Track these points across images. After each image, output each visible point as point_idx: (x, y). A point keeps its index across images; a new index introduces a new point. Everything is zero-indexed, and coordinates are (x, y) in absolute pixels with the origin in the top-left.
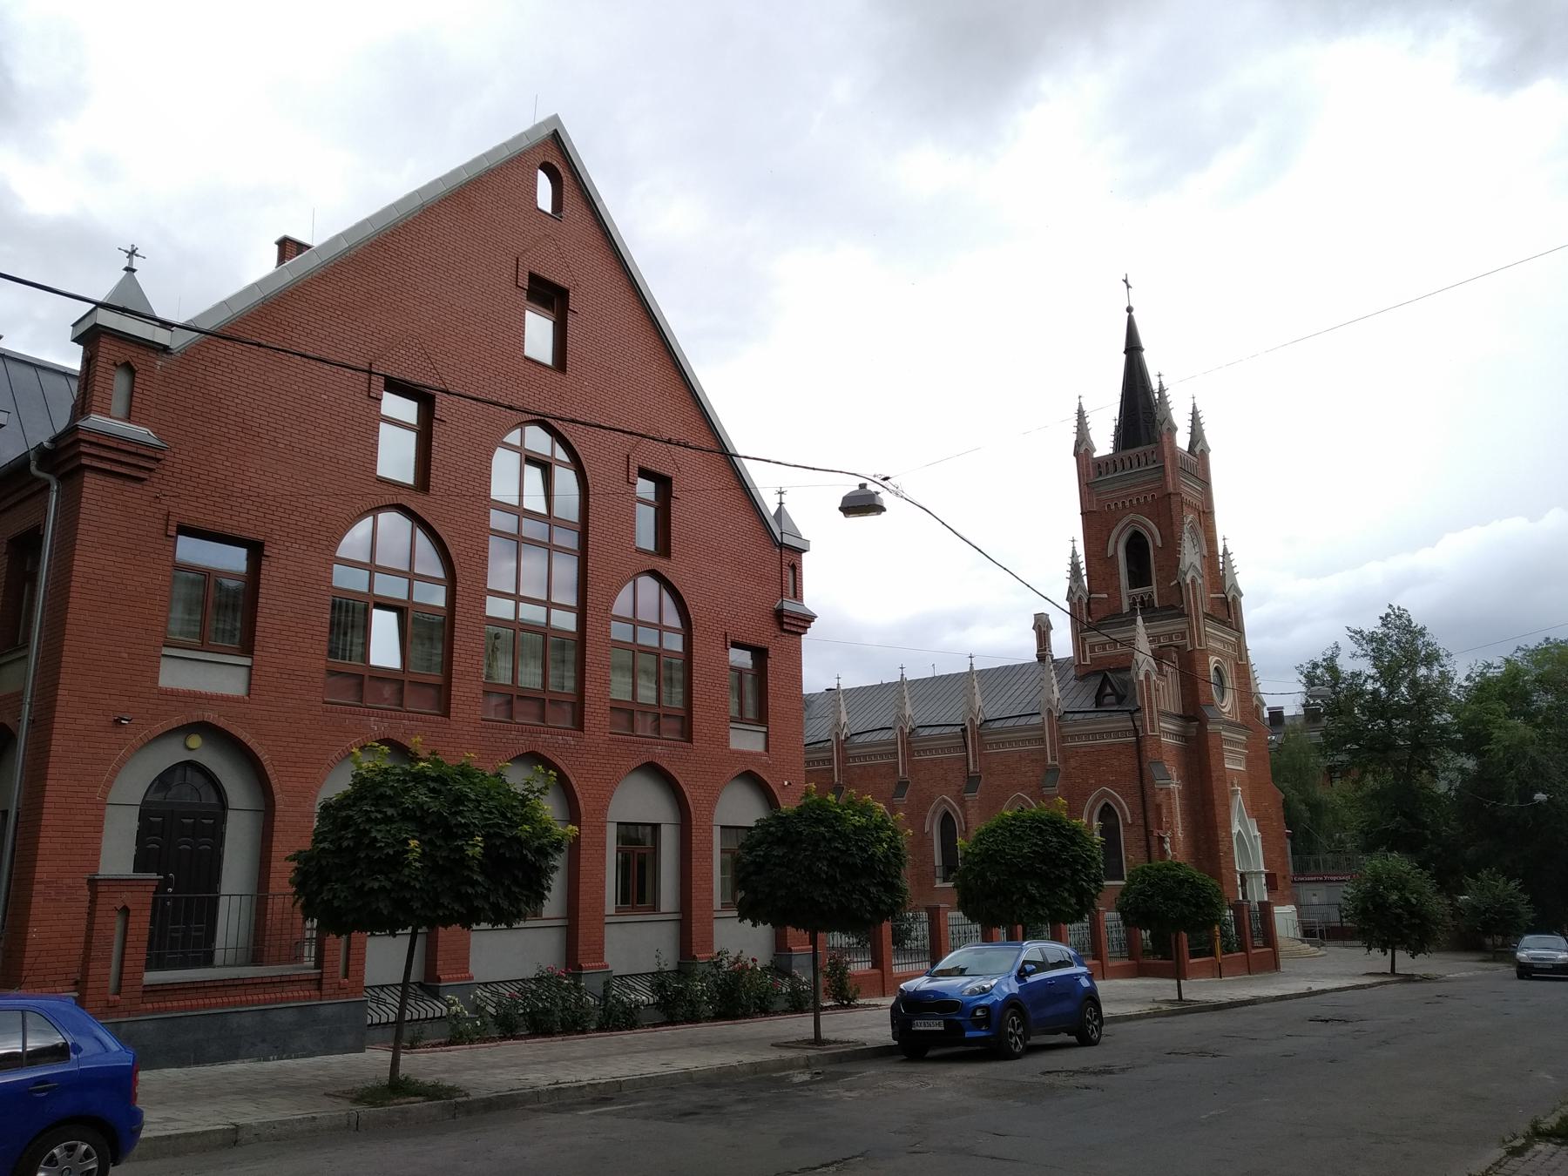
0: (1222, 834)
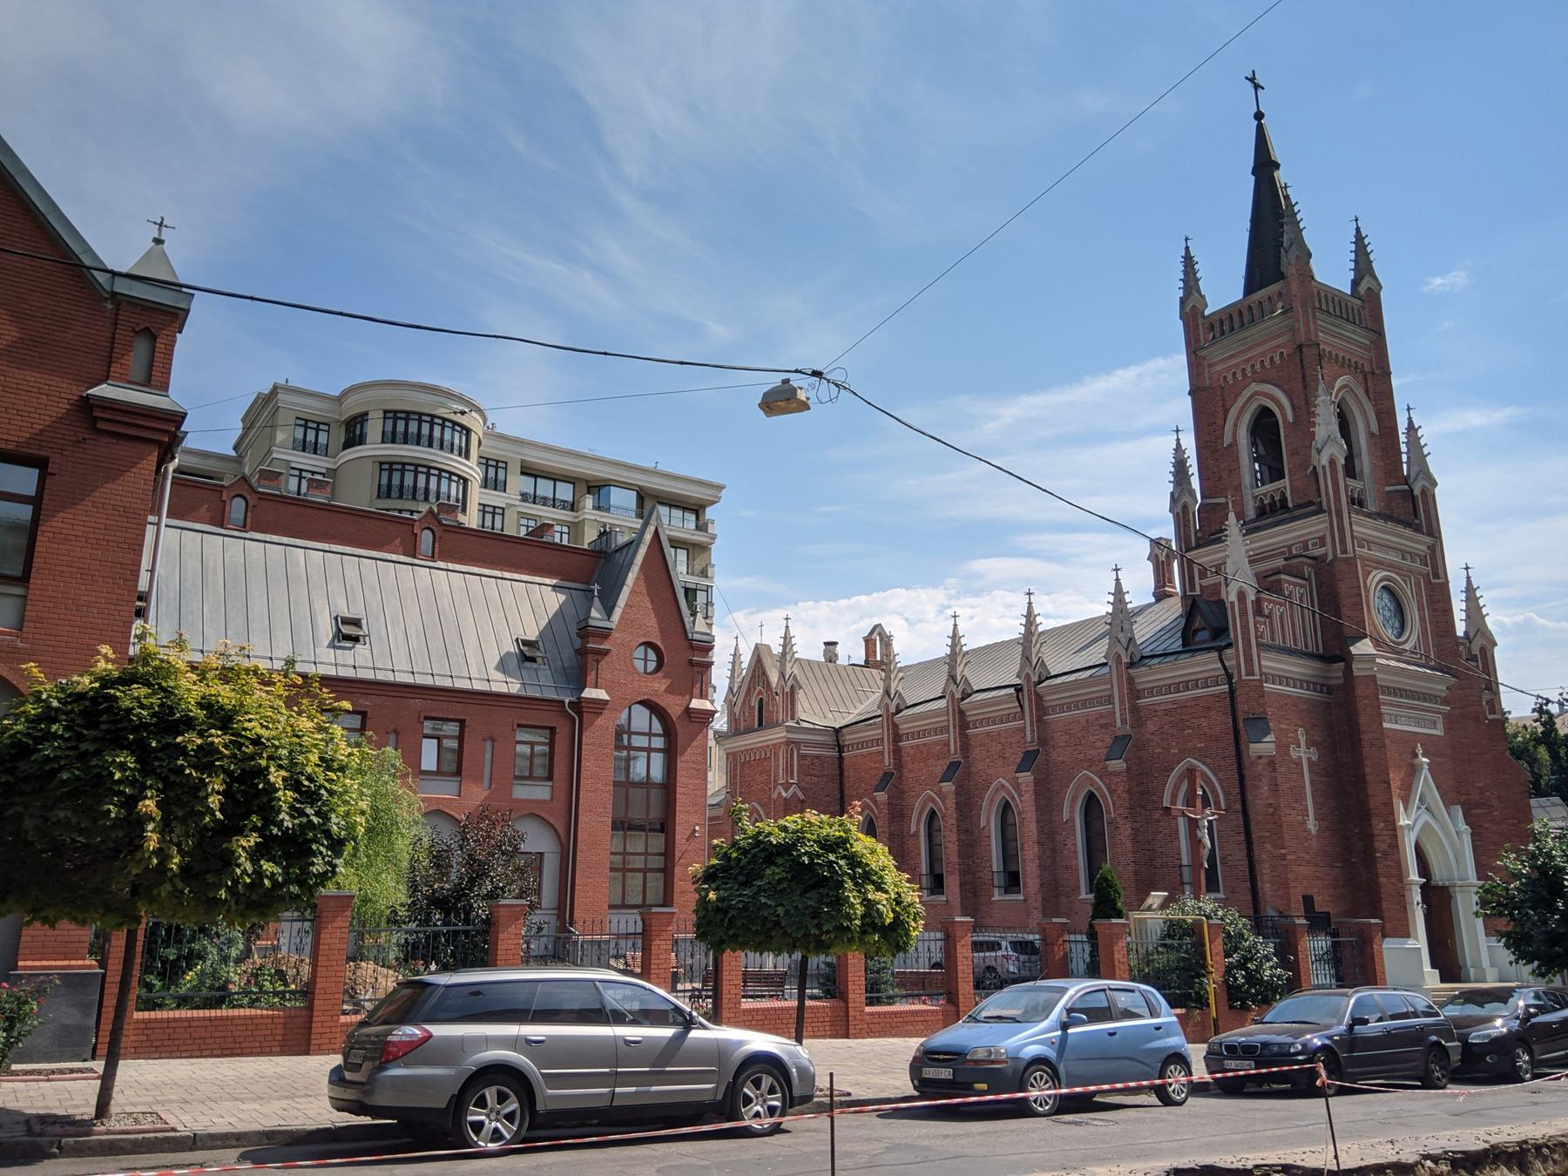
0: (1379, 825)
